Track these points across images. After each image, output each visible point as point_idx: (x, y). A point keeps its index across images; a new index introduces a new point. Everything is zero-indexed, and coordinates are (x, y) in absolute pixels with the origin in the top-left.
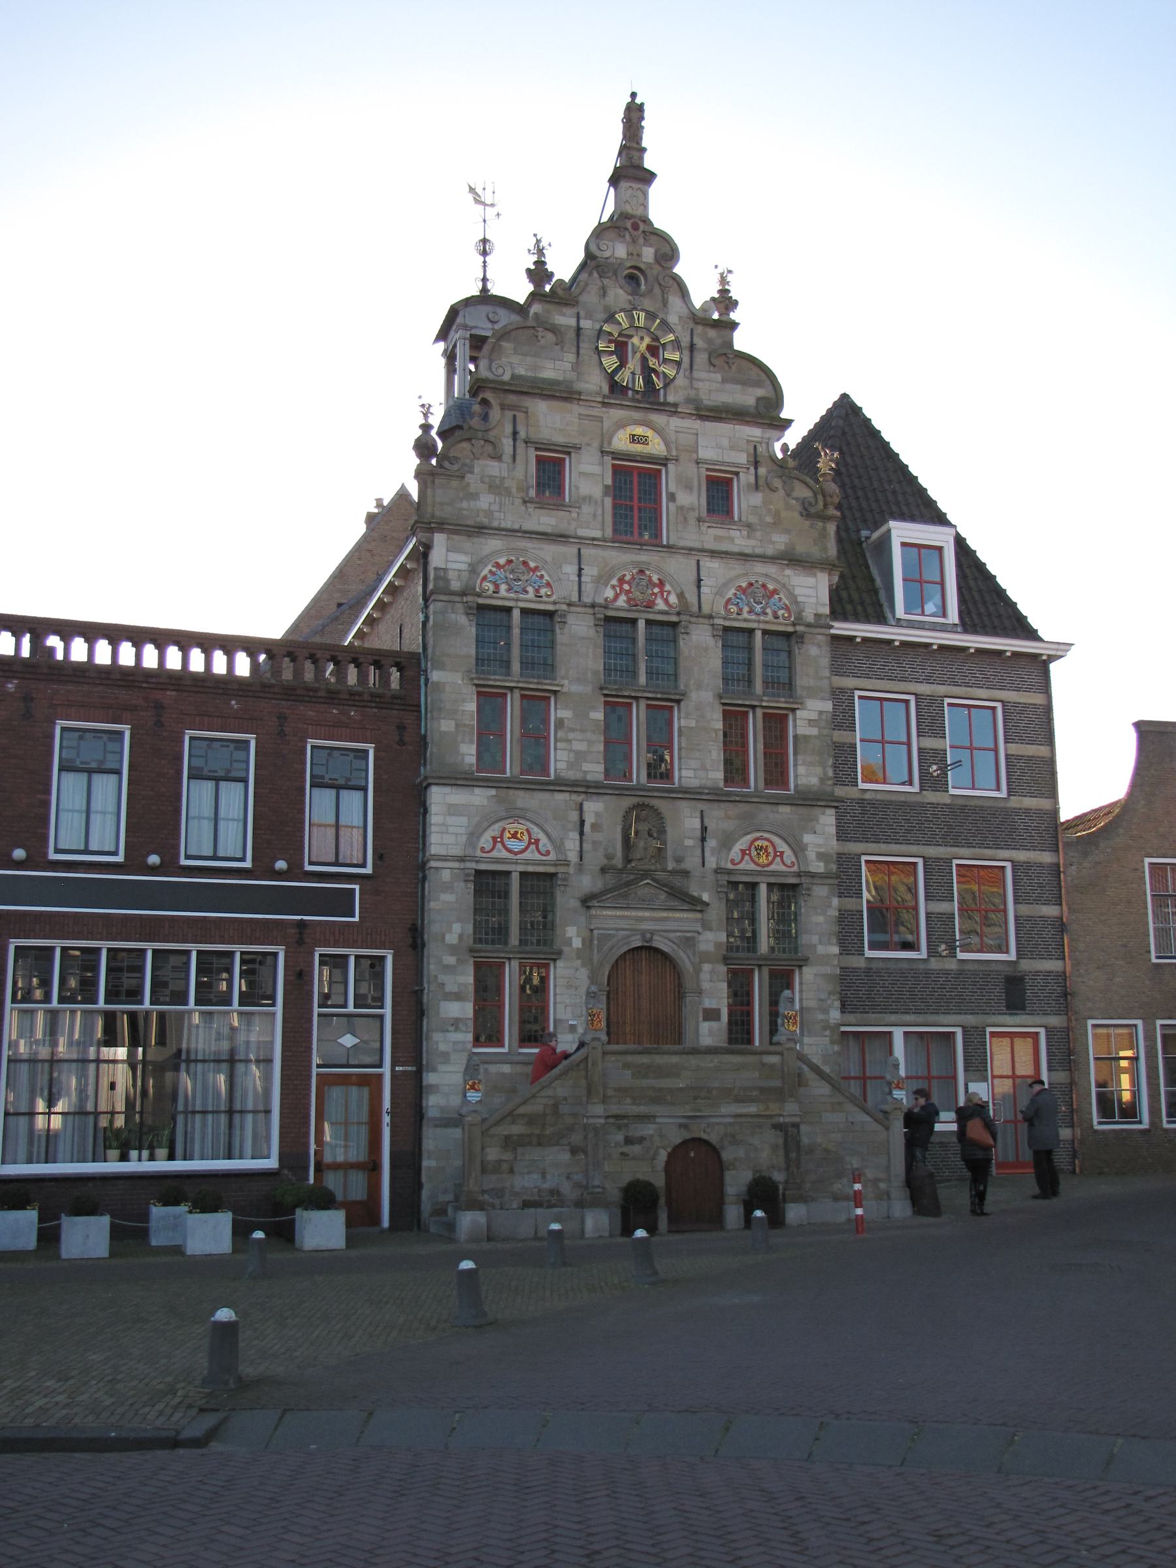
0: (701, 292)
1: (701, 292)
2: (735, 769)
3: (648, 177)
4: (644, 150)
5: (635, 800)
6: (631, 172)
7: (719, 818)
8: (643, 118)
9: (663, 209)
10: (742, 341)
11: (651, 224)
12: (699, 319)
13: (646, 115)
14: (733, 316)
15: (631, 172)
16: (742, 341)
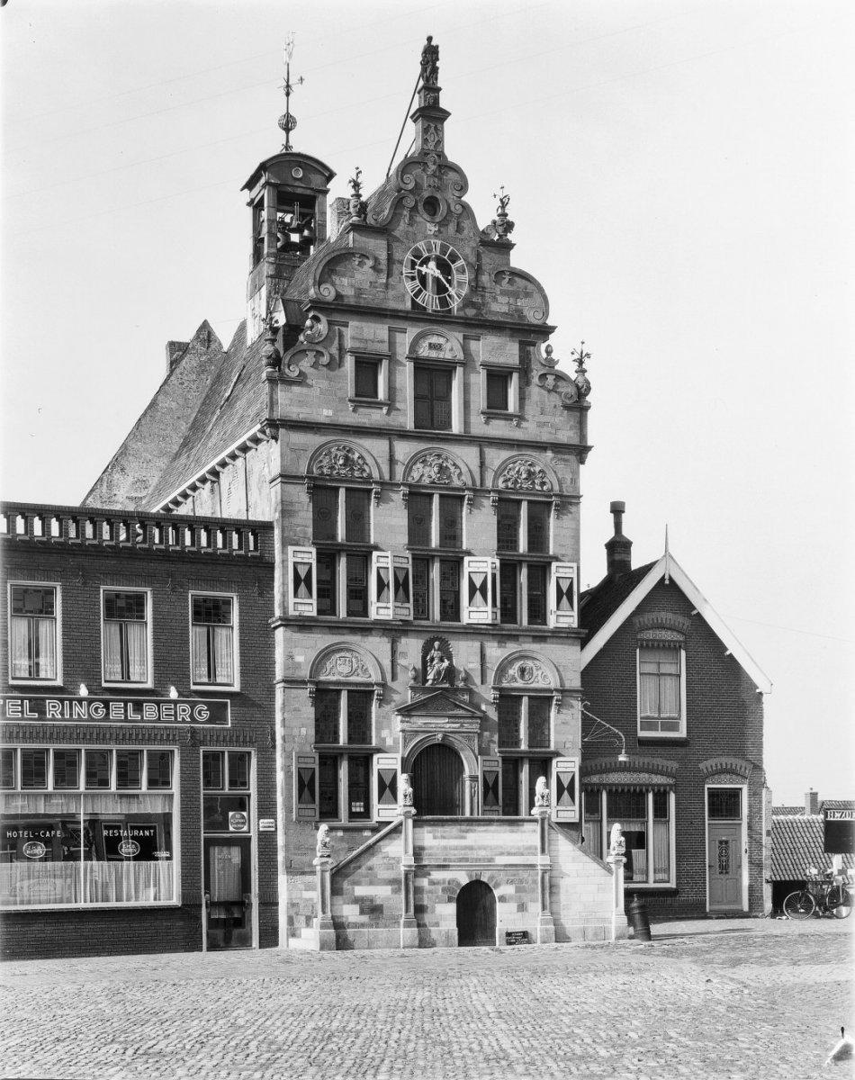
0: (485, 216)
1: (485, 216)
2: (508, 612)
3: (445, 115)
4: (439, 90)
5: (431, 635)
6: (431, 114)
7: (496, 652)
8: (438, 59)
9: (454, 150)
10: (517, 260)
11: (445, 158)
12: (485, 242)
13: (440, 56)
14: (510, 236)
15: (431, 114)
16: (517, 260)
